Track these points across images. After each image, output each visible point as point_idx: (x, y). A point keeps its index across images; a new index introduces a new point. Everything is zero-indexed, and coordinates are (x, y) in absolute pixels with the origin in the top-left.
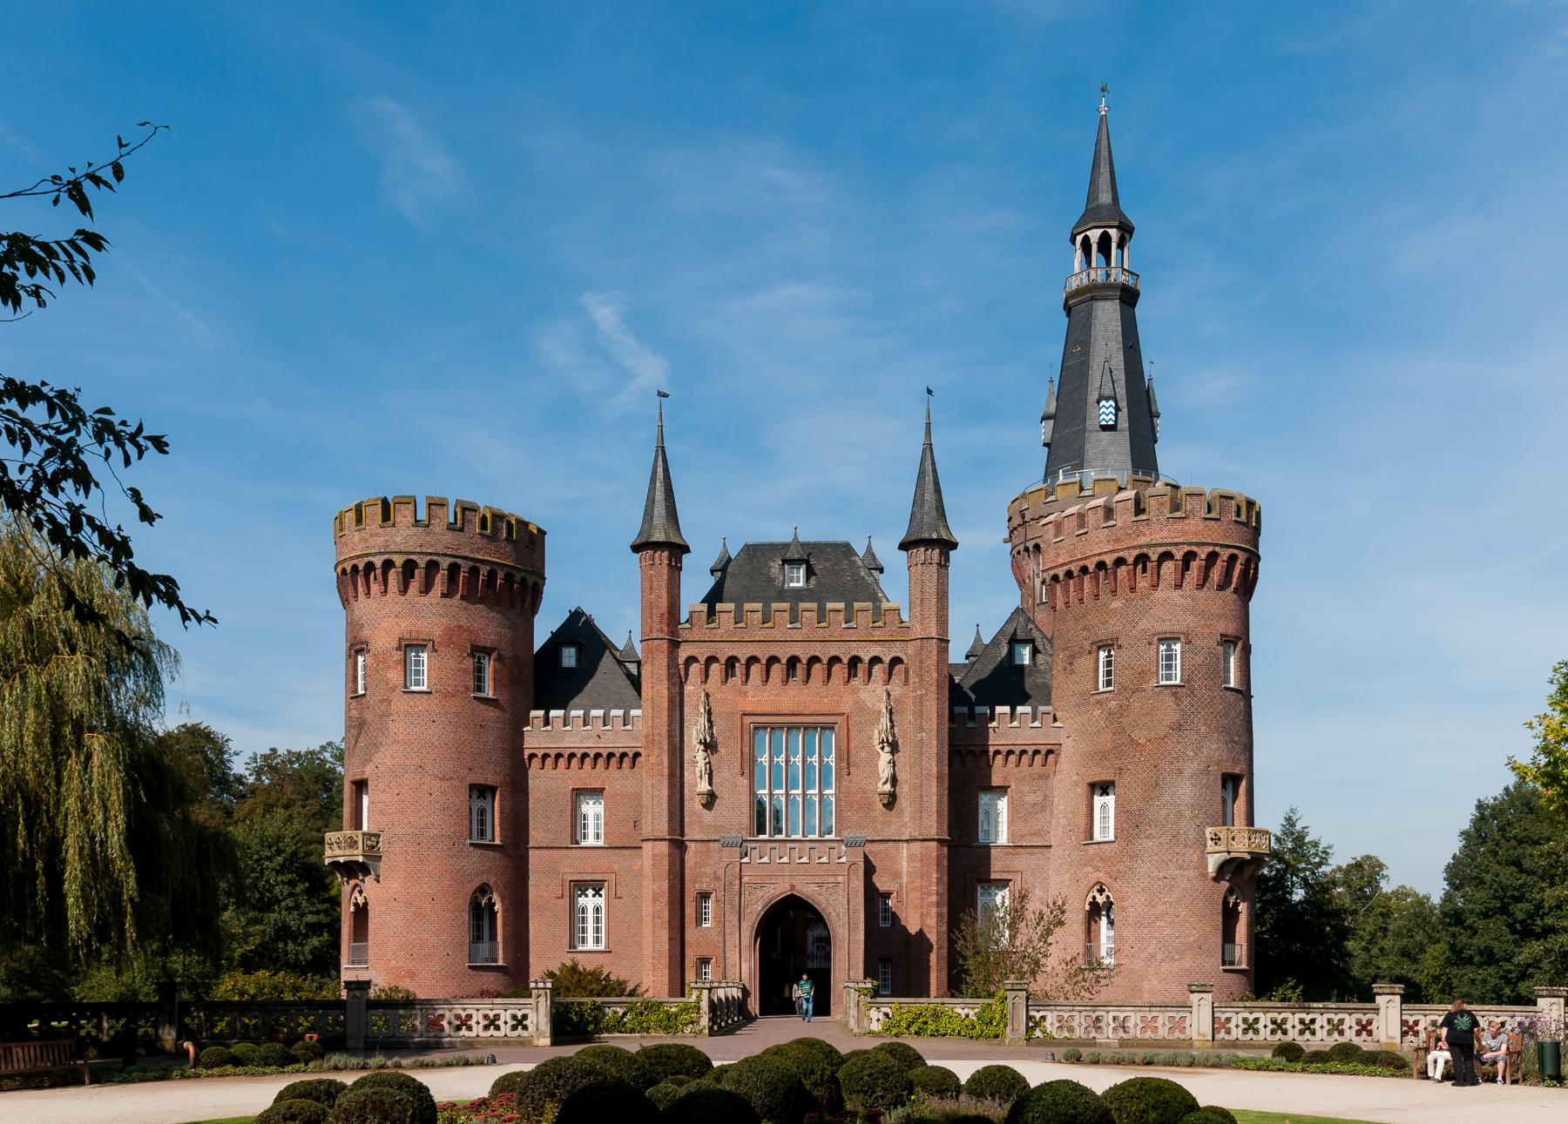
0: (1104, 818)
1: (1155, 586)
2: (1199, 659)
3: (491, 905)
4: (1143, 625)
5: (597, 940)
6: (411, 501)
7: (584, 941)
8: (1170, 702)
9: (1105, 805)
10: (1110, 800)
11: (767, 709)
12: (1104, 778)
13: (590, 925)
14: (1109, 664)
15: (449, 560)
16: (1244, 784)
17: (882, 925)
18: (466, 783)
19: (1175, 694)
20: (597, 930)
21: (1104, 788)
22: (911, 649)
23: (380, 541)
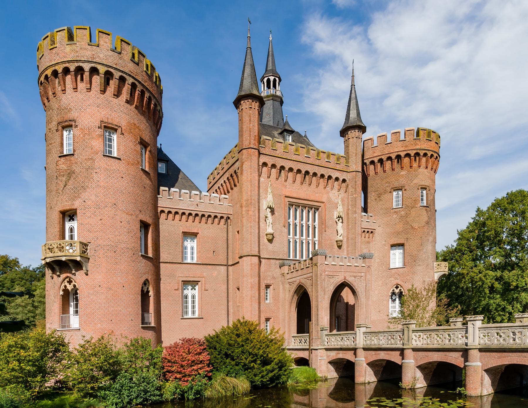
5: (193, 312)
7: (187, 313)
11: (294, 196)
13: (190, 305)
19: (426, 210)
20: (193, 307)
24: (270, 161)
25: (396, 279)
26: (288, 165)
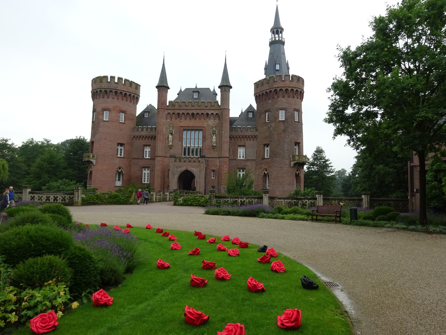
0: (267, 153)
1: (278, 97)
2: (289, 114)
3: (122, 172)
4: (276, 106)
6: (106, 77)
8: (282, 124)
9: (267, 149)
10: (268, 148)
11: (186, 125)
12: (267, 143)
14: (268, 116)
15: (115, 90)
16: (301, 145)
17: (213, 178)
18: (116, 143)
21: (267, 145)
22: (220, 111)
23: (99, 86)
24: (171, 112)
25: (265, 165)
26: (181, 112)
